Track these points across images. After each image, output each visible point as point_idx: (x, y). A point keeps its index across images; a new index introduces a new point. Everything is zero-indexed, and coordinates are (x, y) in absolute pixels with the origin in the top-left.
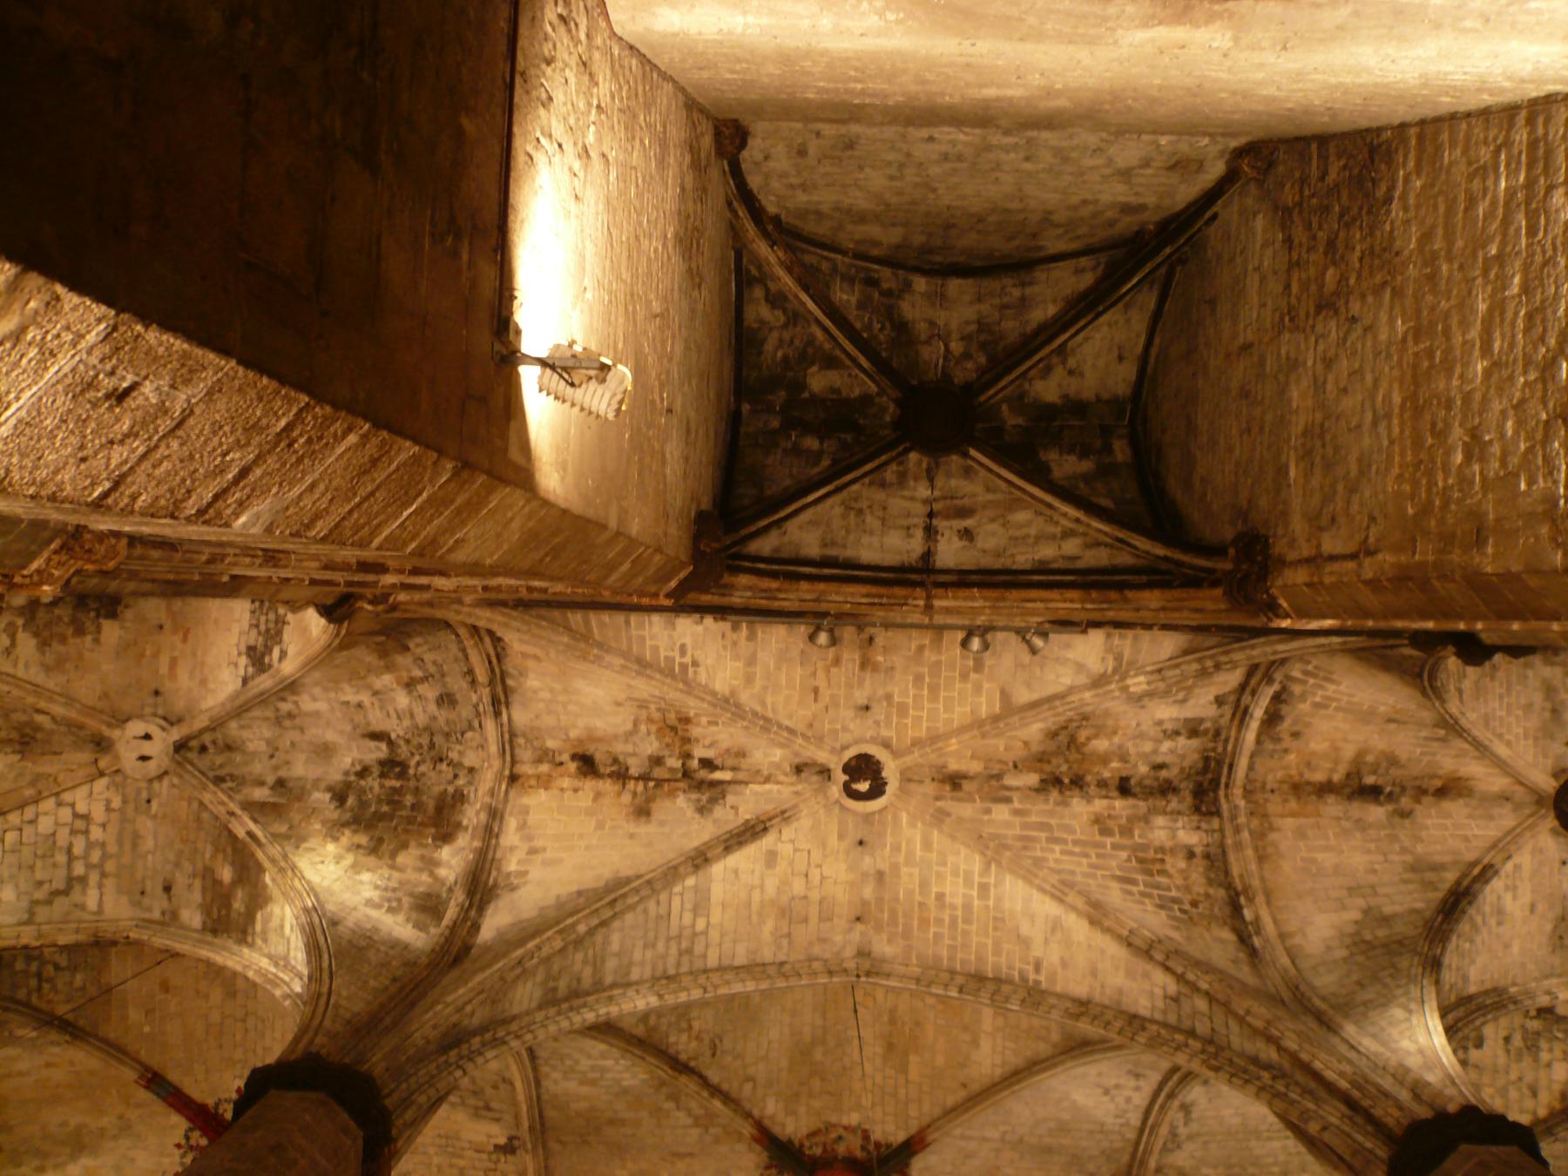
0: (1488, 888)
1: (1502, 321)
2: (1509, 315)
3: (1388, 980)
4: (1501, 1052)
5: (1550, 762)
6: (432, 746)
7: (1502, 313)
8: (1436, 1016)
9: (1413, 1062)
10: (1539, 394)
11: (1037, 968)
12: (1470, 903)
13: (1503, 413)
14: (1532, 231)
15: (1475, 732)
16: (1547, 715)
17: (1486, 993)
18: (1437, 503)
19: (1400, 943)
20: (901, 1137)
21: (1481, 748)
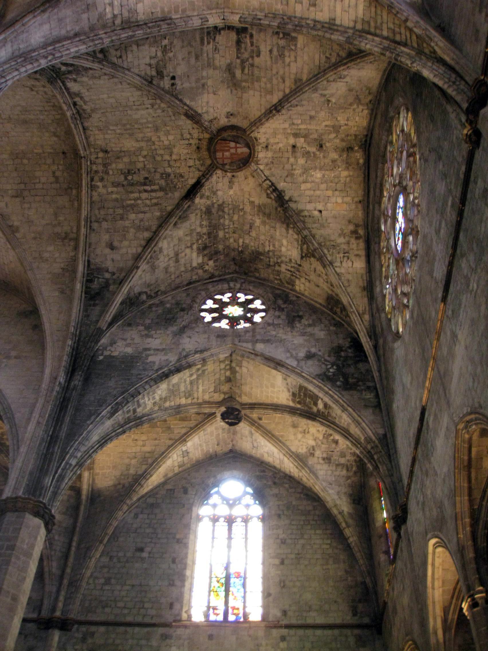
4: (268, 59)
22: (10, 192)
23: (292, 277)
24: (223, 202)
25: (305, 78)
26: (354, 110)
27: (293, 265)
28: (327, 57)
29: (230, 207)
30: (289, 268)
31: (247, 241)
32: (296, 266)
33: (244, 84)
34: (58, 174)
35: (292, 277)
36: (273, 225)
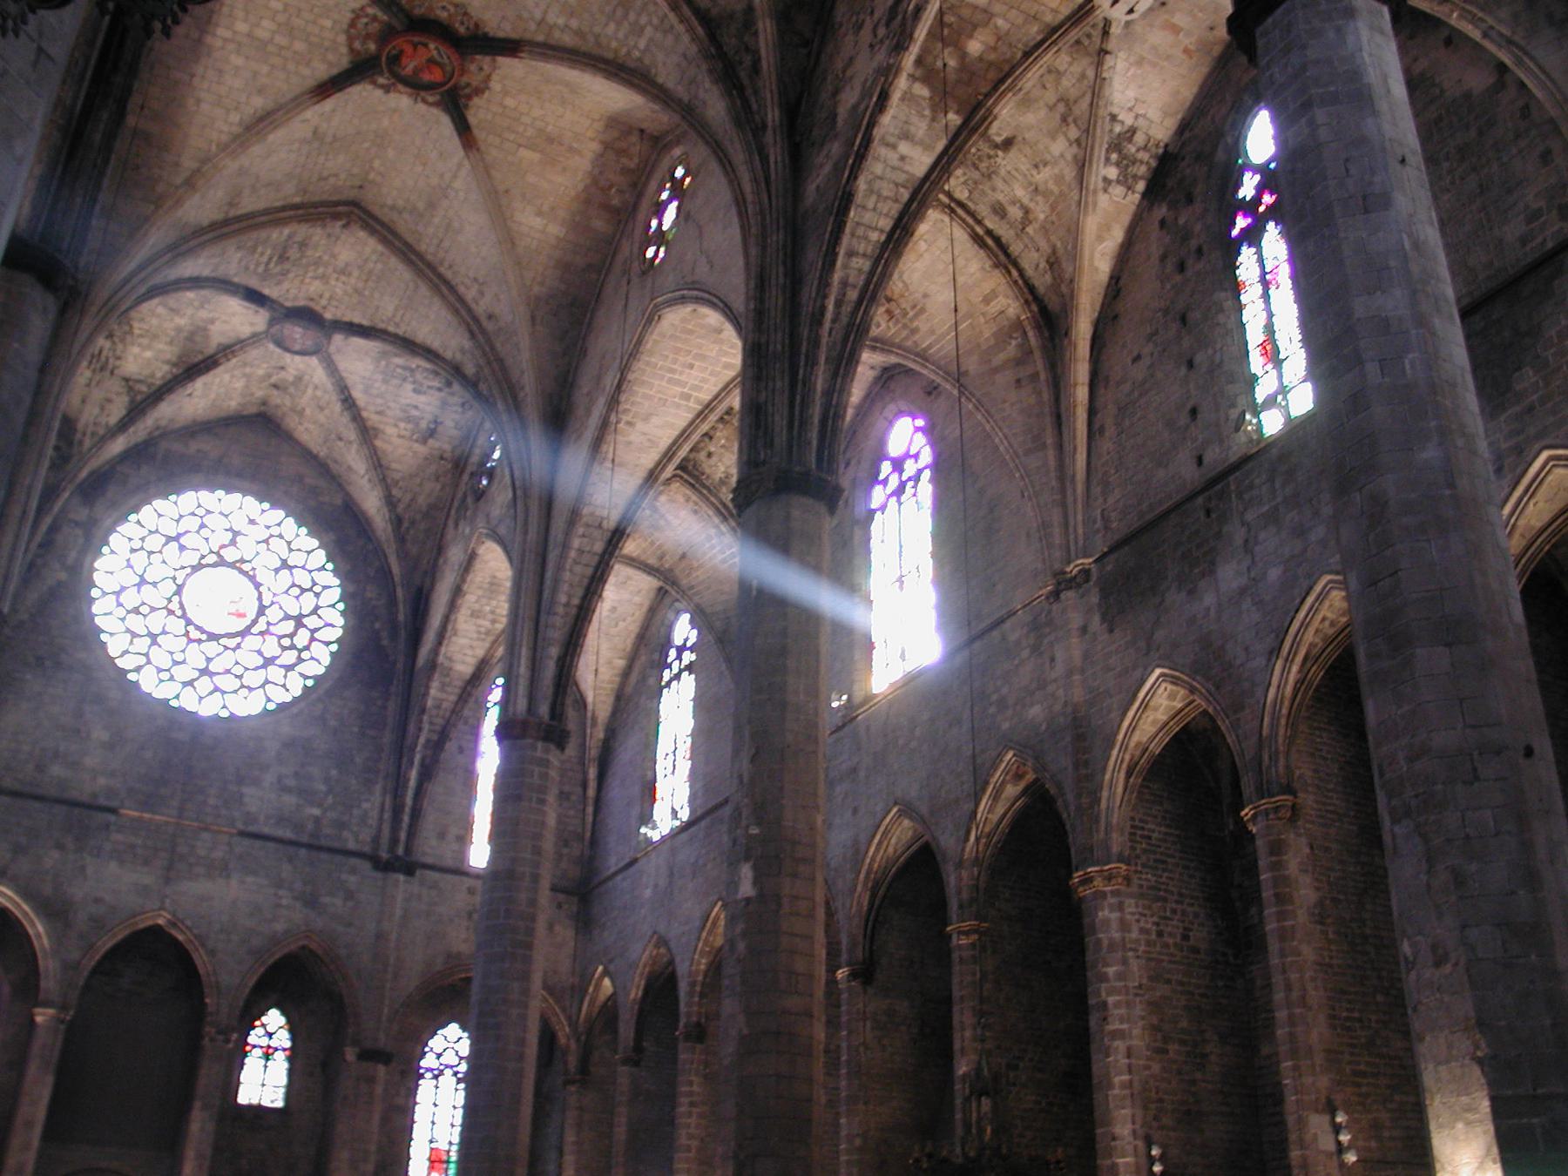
4: (408, 401)
6: (977, 168)
11: (629, 423)
20: (472, 120)
22: (325, 125)
25: (378, 443)
27: (111, 361)
28: (397, 482)
30: (105, 353)
32: (110, 366)
33: (383, 363)
34: (332, 180)
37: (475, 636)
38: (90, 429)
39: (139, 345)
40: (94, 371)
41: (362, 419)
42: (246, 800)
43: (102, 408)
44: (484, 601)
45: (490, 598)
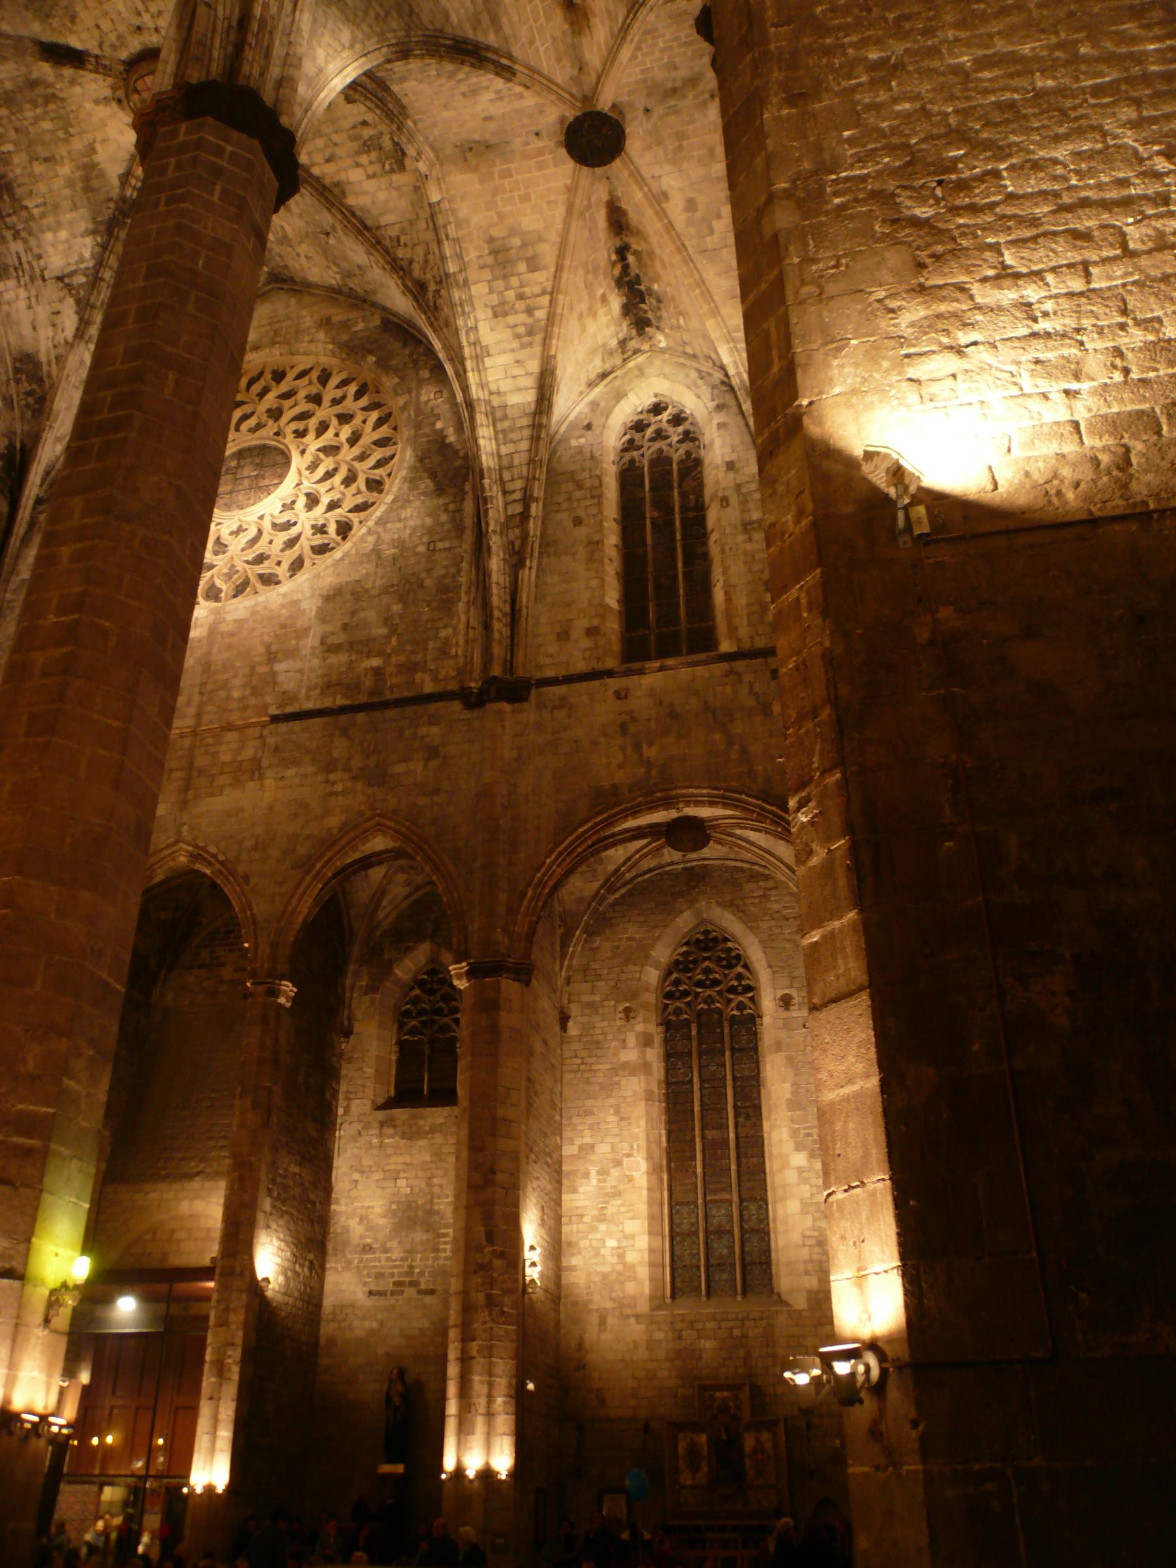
0: (492, 76)
1: (1011, 76)
2: (1015, 82)
3: (372, 14)
4: (351, 121)
5: (625, 98)
7: (1018, 74)
8: (360, 71)
9: (308, 67)
10: (935, 131)
12: (473, 66)
13: (918, 97)
14: (1098, 91)
15: (636, 25)
16: (670, 85)
17: (398, 101)
18: (829, 41)
19: (412, 12)
21: (622, 33)
23: (12, 269)
24: (63, 100)
25: (351, 201)
26: (328, 267)
27: (34, 263)
28: (398, 238)
29: (62, 111)
30: (24, 260)
31: (16, 159)
35: (12, 269)
36: (78, 203)
37: (516, 344)
38: (53, 353)
39: (49, 229)
40: (26, 289)
41: (317, 179)
42: (281, 678)
43: (54, 325)
44: (499, 285)
45: (505, 277)
